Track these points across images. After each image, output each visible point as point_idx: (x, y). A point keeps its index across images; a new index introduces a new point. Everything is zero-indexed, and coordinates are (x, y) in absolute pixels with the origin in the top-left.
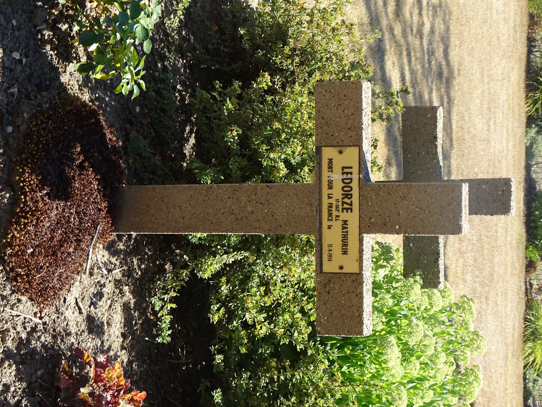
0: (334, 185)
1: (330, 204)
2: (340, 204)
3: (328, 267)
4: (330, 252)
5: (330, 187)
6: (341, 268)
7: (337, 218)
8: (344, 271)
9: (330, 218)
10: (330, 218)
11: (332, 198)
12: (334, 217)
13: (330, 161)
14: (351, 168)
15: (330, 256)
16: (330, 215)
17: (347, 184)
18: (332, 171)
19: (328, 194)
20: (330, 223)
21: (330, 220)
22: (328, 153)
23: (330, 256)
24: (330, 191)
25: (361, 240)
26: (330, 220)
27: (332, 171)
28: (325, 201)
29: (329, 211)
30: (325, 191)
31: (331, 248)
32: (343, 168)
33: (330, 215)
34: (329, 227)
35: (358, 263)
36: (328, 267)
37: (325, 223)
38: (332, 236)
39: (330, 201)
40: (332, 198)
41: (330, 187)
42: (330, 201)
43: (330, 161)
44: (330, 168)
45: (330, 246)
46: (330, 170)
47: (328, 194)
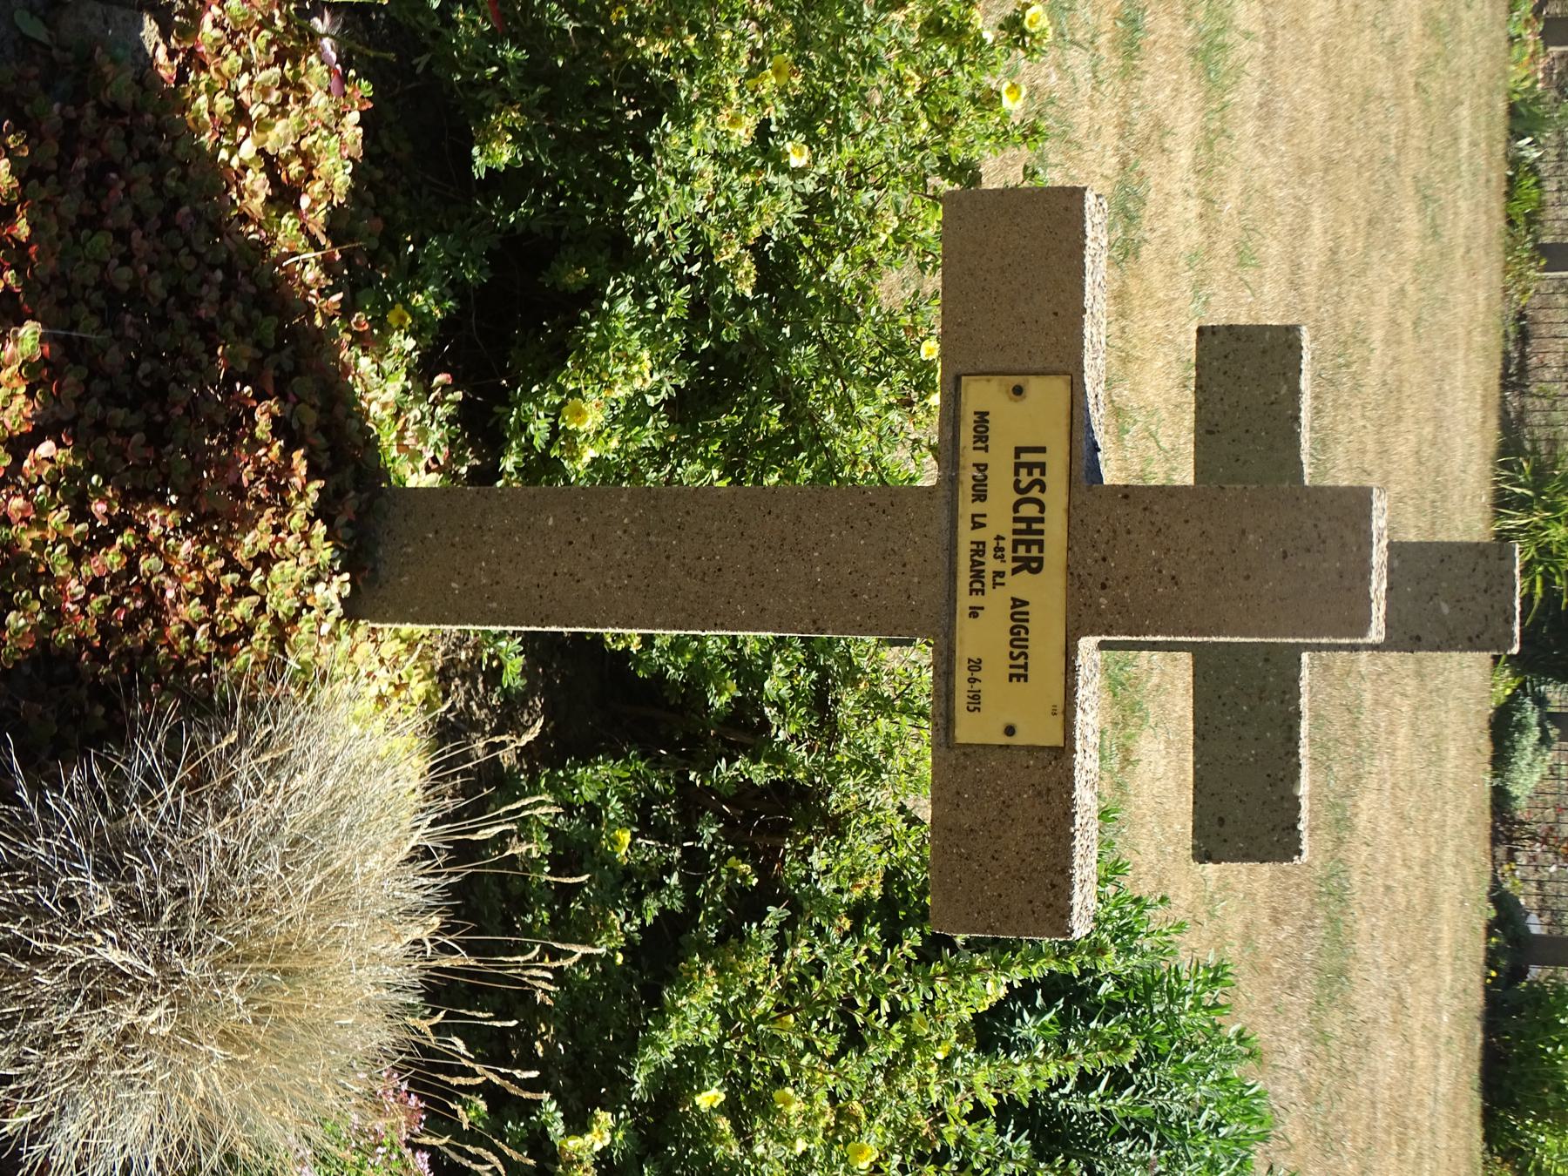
0: (992, 487)
1: (978, 543)
2: (1007, 545)
3: (969, 730)
4: (976, 686)
6: (1010, 731)
7: (998, 580)
8: (1019, 739)
9: (977, 586)
10: (977, 586)
11: (983, 525)
12: (988, 580)
13: (982, 417)
14: (1042, 450)
15: (975, 697)
16: (977, 575)
17: (1028, 491)
18: (986, 449)
19: (974, 516)
20: (976, 600)
21: (977, 591)
22: (980, 394)
23: (975, 697)
24: (978, 507)
25: (1070, 653)
26: (977, 591)
27: (986, 449)
28: (966, 536)
29: (974, 563)
30: (967, 507)
31: (976, 675)
32: (1019, 451)
34: (974, 612)
35: (1060, 718)
36: (969, 730)
37: (965, 600)
38: (981, 636)
39: (979, 535)
40: (983, 525)
41: (980, 495)
42: (979, 535)
43: (982, 417)
44: (981, 437)
45: (975, 665)
46: (979, 444)
47: (974, 516)
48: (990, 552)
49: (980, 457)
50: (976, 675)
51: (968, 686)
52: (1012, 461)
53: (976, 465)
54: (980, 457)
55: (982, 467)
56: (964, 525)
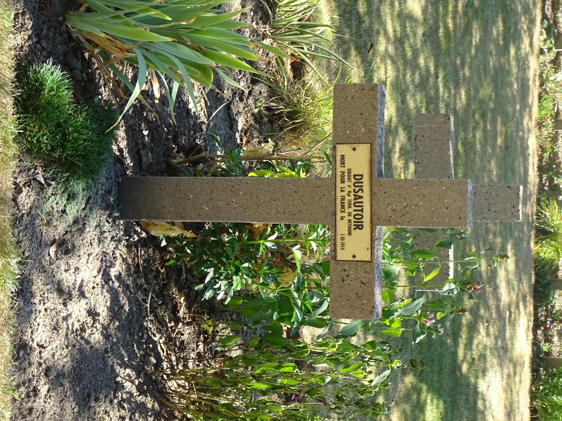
2: (352, 197)
3: (342, 255)
4: (343, 241)
5: (343, 182)
6: (354, 257)
8: (358, 258)
10: (343, 210)
16: (343, 207)
18: (344, 167)
22: (342, 149)
23: (343, 244)
27: (344, 167)
28: (339, 194)
29: (342, 203)
30: (339, 185)
33: (343, 207)
34: (342, 219)
35: (370, 251)
37: (339, 215)
41: (343, 182)
43: (343, 157)
44: (343, 163)
49: (343, 169)
51: (341, 241)
54: (343, 169)
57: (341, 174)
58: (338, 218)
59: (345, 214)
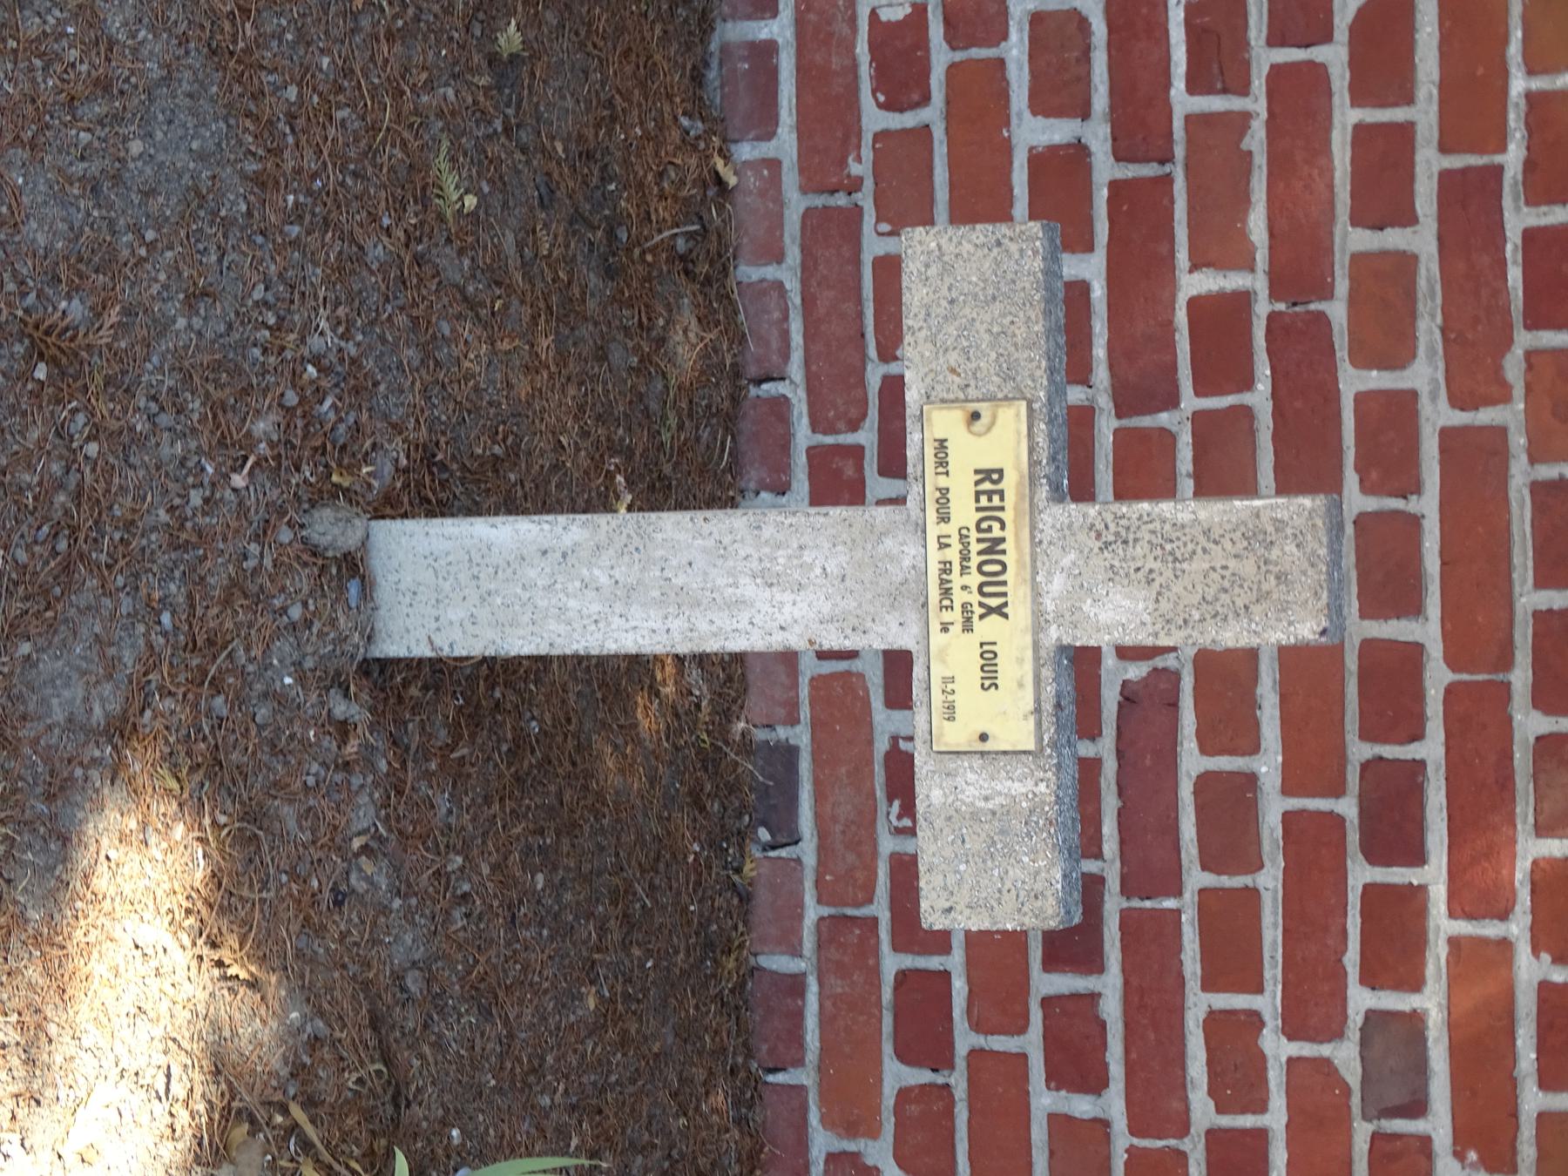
0: (953, 506)
4: (950, 698)
9: (946, 603)
10: (946, 603)
16: (946, 592)
20: (947, 616)
24: (944, 528)
27: (947, 473)
29: (942, 582)
33: (946, 592)
34: (945, 629)
40: (948, 546)
41: (944, 518)
43: (942, 444)
44: (942, 463)
46: (940, 470)
48: (956, 568)
49: (943, 481)
50: (950, 686)
52: (974, 505)
53: (940, 490)
54: (943, 481)
55: (944, 492)
56: (932, 544)
57: (938, 494)
58: (935, 627)
59: (956, 616)
